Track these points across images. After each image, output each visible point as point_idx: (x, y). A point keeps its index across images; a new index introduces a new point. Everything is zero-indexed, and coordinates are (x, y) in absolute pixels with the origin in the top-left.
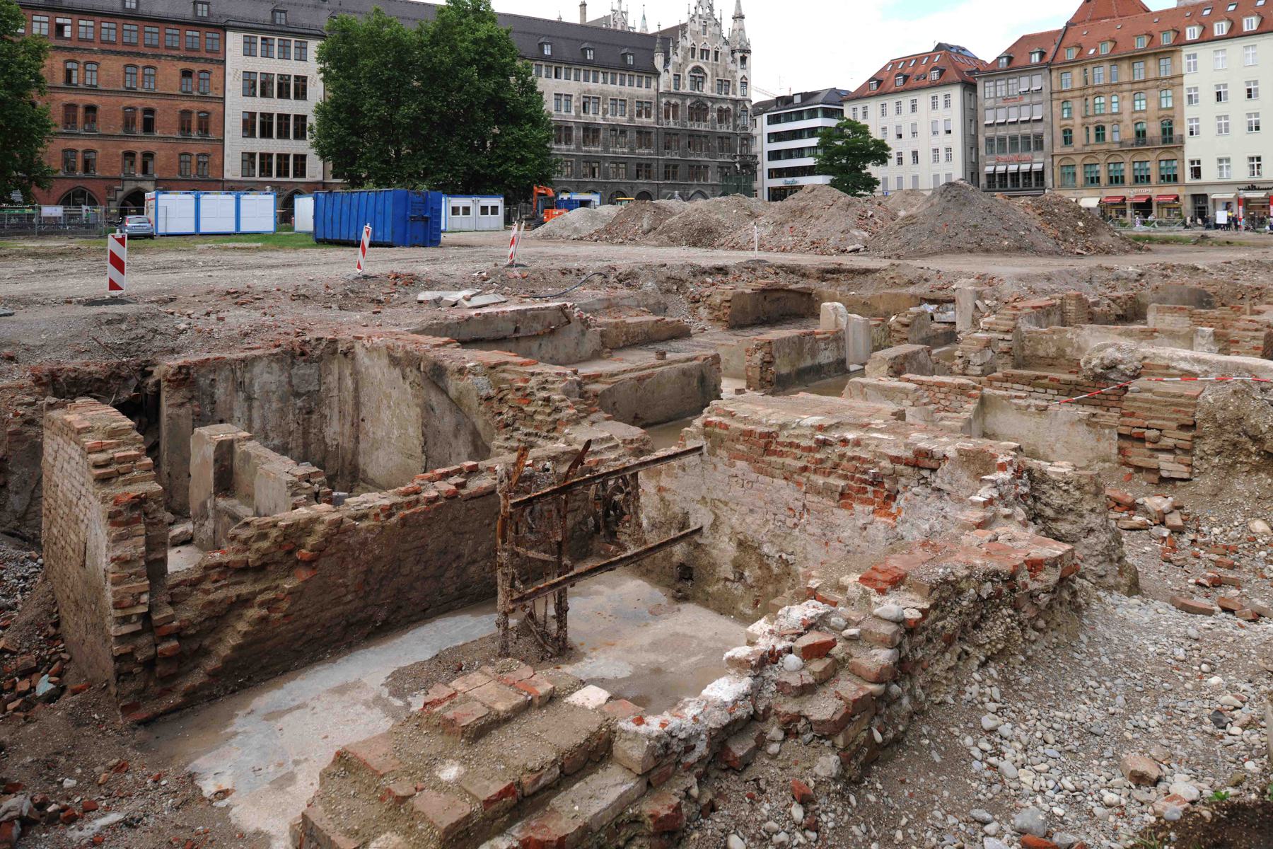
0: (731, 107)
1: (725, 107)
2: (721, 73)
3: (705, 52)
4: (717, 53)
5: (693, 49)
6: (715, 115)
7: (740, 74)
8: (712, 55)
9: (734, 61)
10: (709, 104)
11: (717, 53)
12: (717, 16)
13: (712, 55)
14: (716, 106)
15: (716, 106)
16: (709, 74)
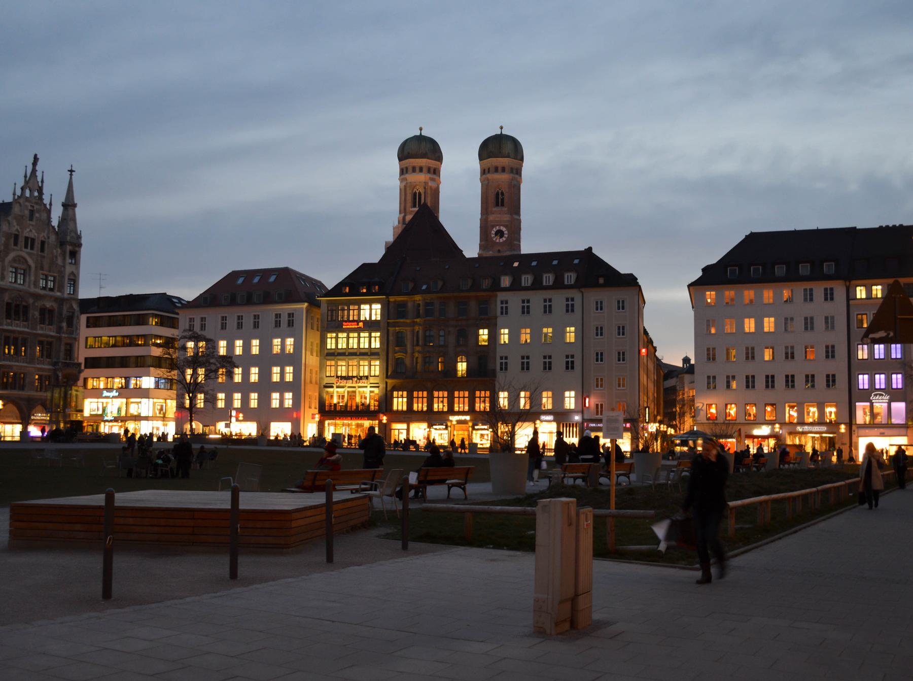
0: (55, 305)
1: (48, 304)
2: (46, 267)
3: (29, 242)
4: (43, 243)
5: (16, 237)
6: (37, 314)
7: (69, 269)
8: (37, 245)
9: (63, 254)
10: (31, 301)
11: (43, 243)
12: (46, 201)
13: (37, 245)
14: (39, 304)
15: (39, 304)
16: (33, 266)
